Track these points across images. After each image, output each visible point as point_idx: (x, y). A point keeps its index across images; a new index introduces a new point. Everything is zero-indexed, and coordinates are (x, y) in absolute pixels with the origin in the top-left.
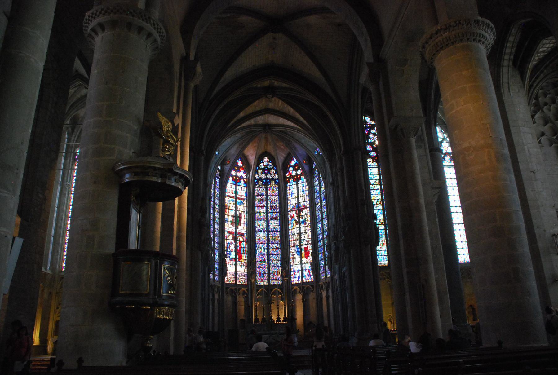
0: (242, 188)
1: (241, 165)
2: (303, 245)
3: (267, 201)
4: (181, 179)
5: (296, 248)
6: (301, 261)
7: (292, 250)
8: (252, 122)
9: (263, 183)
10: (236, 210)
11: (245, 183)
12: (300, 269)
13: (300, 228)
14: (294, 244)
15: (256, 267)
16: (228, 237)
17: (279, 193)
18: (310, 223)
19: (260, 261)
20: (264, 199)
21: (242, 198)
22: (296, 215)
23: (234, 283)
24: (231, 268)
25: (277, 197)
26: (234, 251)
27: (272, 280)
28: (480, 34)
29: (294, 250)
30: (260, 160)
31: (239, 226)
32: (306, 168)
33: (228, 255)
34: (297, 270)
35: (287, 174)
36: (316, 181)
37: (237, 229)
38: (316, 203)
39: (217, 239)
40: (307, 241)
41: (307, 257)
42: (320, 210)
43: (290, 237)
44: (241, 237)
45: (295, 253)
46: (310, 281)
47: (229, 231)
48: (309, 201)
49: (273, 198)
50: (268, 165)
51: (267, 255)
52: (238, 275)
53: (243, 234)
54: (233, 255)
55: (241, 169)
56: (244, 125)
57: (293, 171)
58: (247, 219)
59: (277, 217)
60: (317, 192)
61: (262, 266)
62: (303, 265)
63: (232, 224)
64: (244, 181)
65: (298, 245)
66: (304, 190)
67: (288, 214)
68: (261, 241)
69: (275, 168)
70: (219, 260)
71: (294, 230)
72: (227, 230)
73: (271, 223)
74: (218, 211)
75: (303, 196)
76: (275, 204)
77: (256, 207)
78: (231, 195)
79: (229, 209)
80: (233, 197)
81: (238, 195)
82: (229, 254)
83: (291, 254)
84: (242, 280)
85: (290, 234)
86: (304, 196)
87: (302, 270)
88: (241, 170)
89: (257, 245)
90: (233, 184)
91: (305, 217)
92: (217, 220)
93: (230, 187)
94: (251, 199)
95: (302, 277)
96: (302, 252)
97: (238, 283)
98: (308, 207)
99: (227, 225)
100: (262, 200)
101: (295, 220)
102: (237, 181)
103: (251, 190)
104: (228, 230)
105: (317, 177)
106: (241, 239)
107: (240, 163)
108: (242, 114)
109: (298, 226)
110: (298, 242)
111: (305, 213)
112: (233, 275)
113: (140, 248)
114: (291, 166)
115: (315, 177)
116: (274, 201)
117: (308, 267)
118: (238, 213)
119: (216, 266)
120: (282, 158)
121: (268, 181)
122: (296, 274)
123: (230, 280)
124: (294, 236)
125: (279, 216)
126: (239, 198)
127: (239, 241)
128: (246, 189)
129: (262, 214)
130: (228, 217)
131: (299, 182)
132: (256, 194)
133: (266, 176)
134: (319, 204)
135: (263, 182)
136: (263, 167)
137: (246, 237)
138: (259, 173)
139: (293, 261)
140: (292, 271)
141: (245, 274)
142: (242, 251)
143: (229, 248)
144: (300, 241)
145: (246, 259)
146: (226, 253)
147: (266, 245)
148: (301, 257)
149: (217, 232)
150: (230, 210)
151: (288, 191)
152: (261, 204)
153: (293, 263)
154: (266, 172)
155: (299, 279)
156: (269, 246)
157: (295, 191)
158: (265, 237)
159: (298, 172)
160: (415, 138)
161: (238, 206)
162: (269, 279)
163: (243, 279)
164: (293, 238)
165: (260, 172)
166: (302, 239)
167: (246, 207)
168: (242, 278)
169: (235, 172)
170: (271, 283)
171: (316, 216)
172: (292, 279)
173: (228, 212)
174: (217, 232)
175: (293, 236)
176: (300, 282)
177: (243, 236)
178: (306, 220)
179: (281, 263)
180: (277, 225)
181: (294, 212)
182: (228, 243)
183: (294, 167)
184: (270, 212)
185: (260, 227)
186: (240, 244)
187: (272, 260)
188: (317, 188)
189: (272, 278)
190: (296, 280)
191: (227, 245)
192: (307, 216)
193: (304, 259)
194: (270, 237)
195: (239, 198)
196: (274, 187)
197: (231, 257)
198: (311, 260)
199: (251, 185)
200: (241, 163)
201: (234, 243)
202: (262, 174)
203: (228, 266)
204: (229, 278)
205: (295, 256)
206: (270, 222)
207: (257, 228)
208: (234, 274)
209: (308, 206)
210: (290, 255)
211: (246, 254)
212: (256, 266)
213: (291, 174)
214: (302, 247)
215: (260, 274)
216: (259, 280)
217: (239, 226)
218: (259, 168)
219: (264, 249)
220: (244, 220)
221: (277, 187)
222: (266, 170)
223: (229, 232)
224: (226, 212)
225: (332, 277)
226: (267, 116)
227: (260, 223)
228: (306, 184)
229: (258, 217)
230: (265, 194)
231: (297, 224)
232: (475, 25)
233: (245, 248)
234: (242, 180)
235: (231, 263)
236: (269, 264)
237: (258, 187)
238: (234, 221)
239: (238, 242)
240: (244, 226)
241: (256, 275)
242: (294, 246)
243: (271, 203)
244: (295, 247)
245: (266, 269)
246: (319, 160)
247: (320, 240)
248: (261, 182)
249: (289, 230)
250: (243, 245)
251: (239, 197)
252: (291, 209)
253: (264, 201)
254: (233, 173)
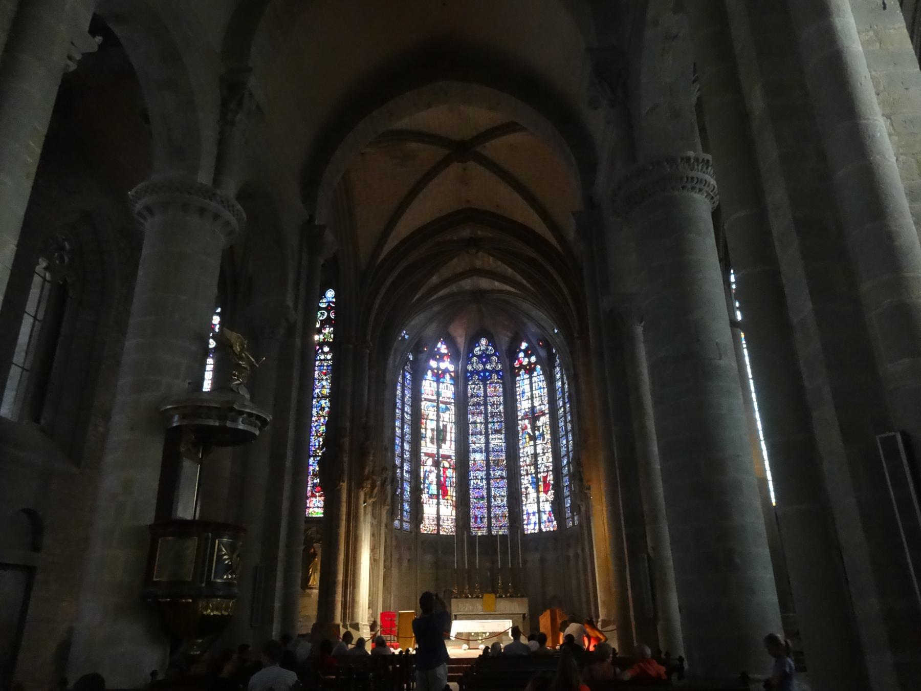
0: (447, 386)
1: (446, 351)
2: (540, 473)
3: (485, 405)
4: (251, 419)
5: (530, 477)
6: (538, 498)
7: (524, 479)
8: (454, 288)
9: (480, 378)
10: (438, 421)
11: (452, 378)
12: (537, 511)
13: (535, 446)
14: (527, 470)
15: (470, 508)
16: (426, 461)
17: (504, 392)
18: (550, 438)
19: (476, 498)
20: (482, 402)
21: (447, 402)
22: (529, 426)
23: (435, 533)
24: (429, 510)
25: (502, 398)
26: (435, 483)
27: (495, 528)
28: (693, 178)
29: (527, 479)
30: (473, 342)
31: (443, 445)
32: (543, 353)
33: (426, 490)
34: (532, 512)
35: (515, 362)
36: (557, 374)
37: (440, 450)
38: (558, 407)
39: (407, 465)
40: (546, 466)
41: (546, 492)
42: (563, 418)
43: (522, 460)
44: (447, 461)
45: (529, 485)
46: (552, 529)
48: (549, 403)
49: (495, 399)
50: (487, 349)
51: (487, 489)
52: (441, 521)
53: (449, 457)
54: (434, 489)
55: (446, 357)
56: (441, 293)
57: (524, 358)
58: (455, 433)
59: (501, 429)
60: (560, 390)
61: (479, 506)
62: (541, 504)
63: (432, 442)
64: (451, 375)
65: (533, 472)
66: (541, 386)
67: (518, 425)
68: (478, 466)
69: (497, 354)
70: (410, 497)
71: (526, 449)
73: (493, 439)
74: (410, 423)
75: (539, 397)
76: (498, 409)
77: (469, 414)
78: (430, 397)
79: (427, 419)
81: (441, 398)
82: (428, 489)
83: (523, 486)
84: (448, 527)
85: (521, 455)
86: (541, 396)
87: (539, 512)
88: (446, 360)
89: (471, 472)
90: (433, 381)
91: (543, 430)
92: (408, 437)
93: (429, 385)
94: (462, 403)
95: (540, 523)
96: (540, 483)
97: (441, 533)
98: (547, 413)
99: (425, 443)
100: (478, 404)
101: (528, 434)
102: (439, 376)
103: (461, 387)
105: (558, 366)
106: (446, 465)
107: (443, 349)
108: (435, 279)
109: (532, 443)
110: (532, 467)
111: (543, 423)
112: (434, 521)
113: (200, 516)
114: (521, 350)
115: (556, 367)
116: (497, 405)
117: (547, 507)
118: (441, 424)
119: (406, 507)
120: (507, 339)
121: (487, 374)
122: (530, 518)
123: (428, 530)
124: (527, 458)
125: (505, 428)
126: (443, 403)
127: (444, 467)
128: (454, 388)
129: (478, 425)
130: (426, 431)
131: (533, 375)
132: (469, 395)
133: (484, 366)
134: (562, 410)
135: (479, 375)
136: (479, 353)
137: (454, 461)
138: (473, 362)
139: (526, 498)
140: (525, 513)
141: (452, 519)
142: (448, 483)
143: (428, 479)
144: (536, 468)
145: (454, 494)
146: (422, 487)
147: (484, 473)
148: (538, 492)
149: (407, 456)
150: (428, 421)
151: (517, 389)
152: (477, 409)
153: (527, 501)
154: (484, 360)
155: (535, 526)
156: (490, 474)
157: (527, 388)
158: (482, 460)
159: (531, 360)
160: (643, 324)
161: (441, 414)
162: (489, 527)
163: (449, 527)
164: (526, 462)
165: (475, 360)
166: (539, 463)
167: (455, 415)
168: (447, 524)
169: (436, 362)
170: (493, 533)
171: (559, 428)
172: (525, 526)
173: (426, 424)
174: (408, 456)
175: (525, 459)
176: (536, 531)
177: (449, 460)
178: (545, 433)
179: (508, 501)
180: (501, 441)
181: (527, 422)
182: (426, 471)
183: (525, 351)
184: (491, 422)
185: (476, 444)
186: (444, 473)
187: (494, 496)
188: (559, 384)
189: (495, 524)
190: (531, 528)
191: (425, 475)
192: (546, 427)
193: (542, 495)
194: (492, 460)
195: (443, 403)
196: (496, 383)
197: (430, 493)
198: (553, 496)
199: (461, 380)
200: (445, 349)
201: (436, 472)
202: (477, 364)
203: (426, 507)
205: (528, 489)
206: (491, 437)
207: (471, 447)
208: (435, 520)
209: (547, 411)
210: (521, 489)
211: (455, 487)
212: (470, 506)
213: (521, 363)
214: (539, 476)
215: (476, 517)
216: (475, 528)
217: (443, 445)
218: (474, 355)
219: (482, 479)
220: (451, 435)
221: (501, 383)
222: (484, 357)
223: (426, 454)
225: (580, 525)
226: (475, 278)
227: (475, 439)
228: (542, 377)
229: (472, 430)
230: (482, 395)
231: (530, 440)
232: (684, 164)
233: (453, 478)
234: (447, 374)
235: (431, 502)
236: (489, 502)
237: (472, 384)
238: (435, 438)
239: (441, 469)
240: (451, 444)
241: (470, 520)
242: (527, 474)
243: (491, 407)
244: (529, 475)
245: (486, 511)
246: (557, 342)
247: (565, 465)
248: (477, 377)
249: (519, 449)
250: (450, 473)
251: (443, 400)
252: (522, 417)
253: (482, 405)
254: (433, 364)
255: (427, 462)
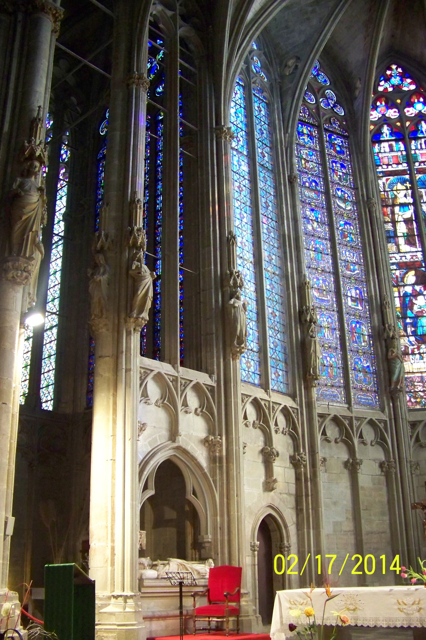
47: (405, 263)
55: (414, 97)
63: (410, 242)
72: (396, 261)
78: (394, 168)
79: (393, 205)
80: (403, 172)
81: (417, 164)
82: (413, 327)
90: (396, 141)
93: (387, 150)
104: (398, 261)
143: (412, 309)
173: (393, 213)
182: (406, 295)
204: (422, 394)
223: (400, 266)
224: (388, 215)
238: (416, 234)
254: (392, 114)
255: (405, 279)
